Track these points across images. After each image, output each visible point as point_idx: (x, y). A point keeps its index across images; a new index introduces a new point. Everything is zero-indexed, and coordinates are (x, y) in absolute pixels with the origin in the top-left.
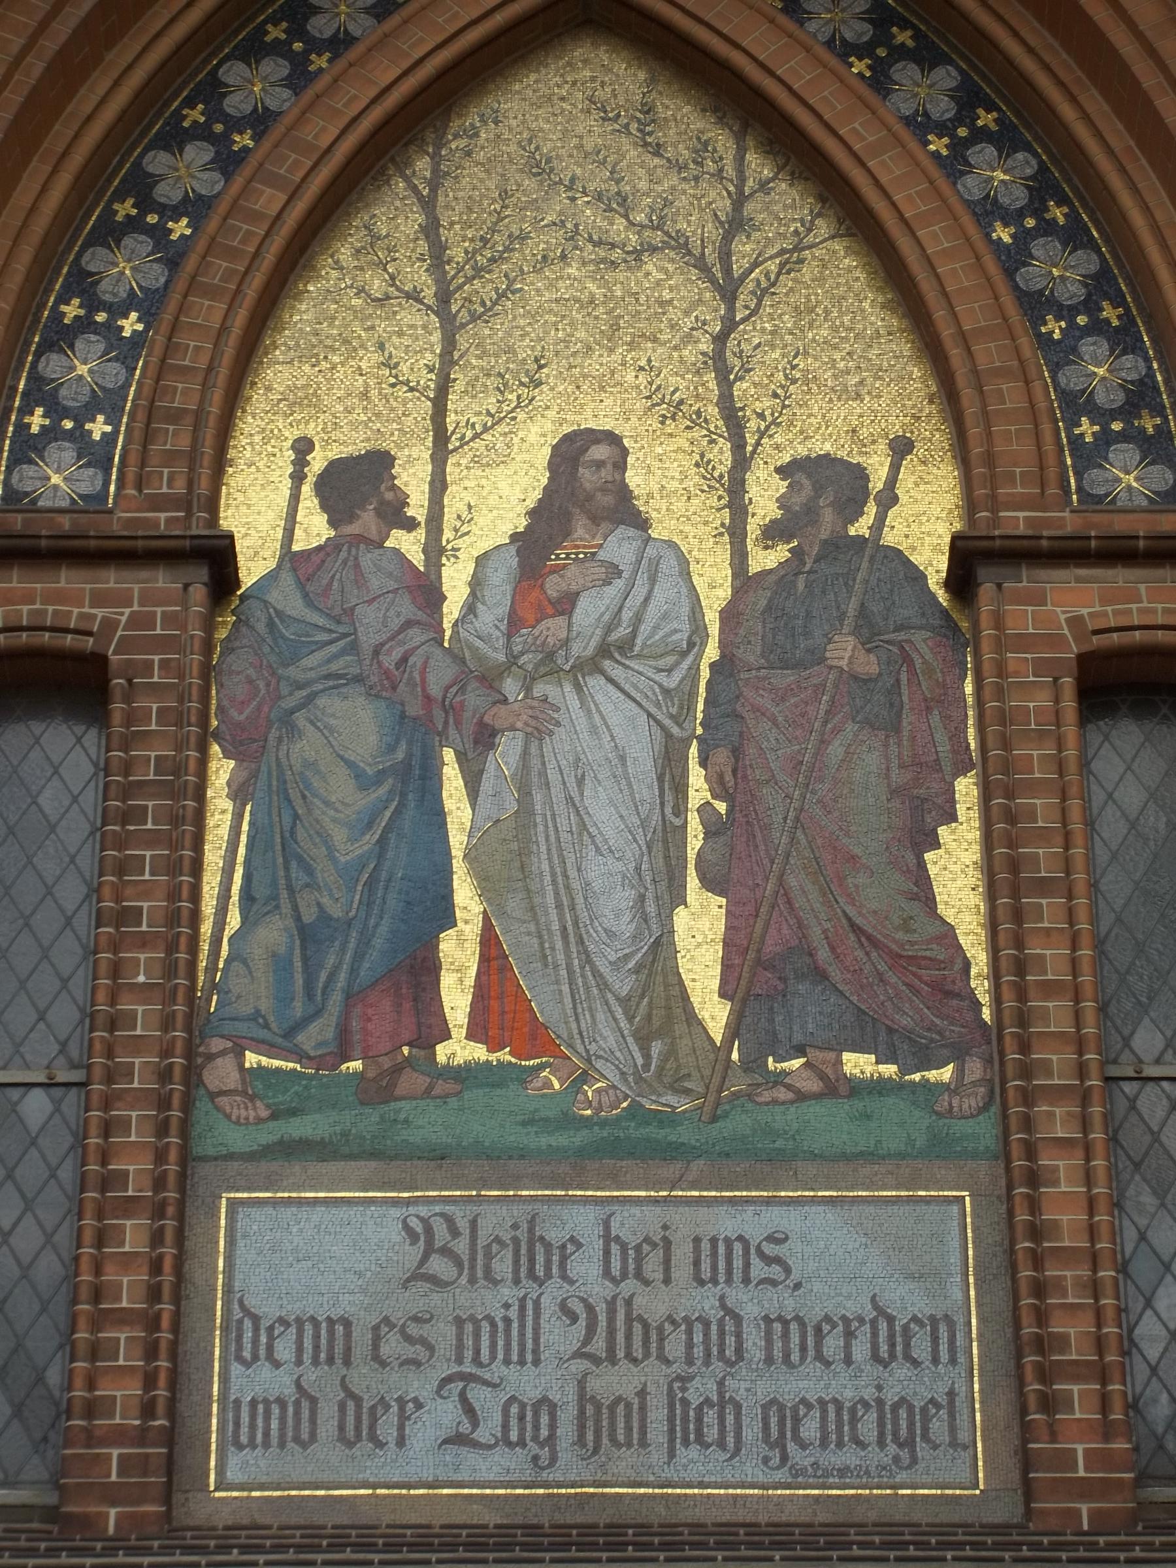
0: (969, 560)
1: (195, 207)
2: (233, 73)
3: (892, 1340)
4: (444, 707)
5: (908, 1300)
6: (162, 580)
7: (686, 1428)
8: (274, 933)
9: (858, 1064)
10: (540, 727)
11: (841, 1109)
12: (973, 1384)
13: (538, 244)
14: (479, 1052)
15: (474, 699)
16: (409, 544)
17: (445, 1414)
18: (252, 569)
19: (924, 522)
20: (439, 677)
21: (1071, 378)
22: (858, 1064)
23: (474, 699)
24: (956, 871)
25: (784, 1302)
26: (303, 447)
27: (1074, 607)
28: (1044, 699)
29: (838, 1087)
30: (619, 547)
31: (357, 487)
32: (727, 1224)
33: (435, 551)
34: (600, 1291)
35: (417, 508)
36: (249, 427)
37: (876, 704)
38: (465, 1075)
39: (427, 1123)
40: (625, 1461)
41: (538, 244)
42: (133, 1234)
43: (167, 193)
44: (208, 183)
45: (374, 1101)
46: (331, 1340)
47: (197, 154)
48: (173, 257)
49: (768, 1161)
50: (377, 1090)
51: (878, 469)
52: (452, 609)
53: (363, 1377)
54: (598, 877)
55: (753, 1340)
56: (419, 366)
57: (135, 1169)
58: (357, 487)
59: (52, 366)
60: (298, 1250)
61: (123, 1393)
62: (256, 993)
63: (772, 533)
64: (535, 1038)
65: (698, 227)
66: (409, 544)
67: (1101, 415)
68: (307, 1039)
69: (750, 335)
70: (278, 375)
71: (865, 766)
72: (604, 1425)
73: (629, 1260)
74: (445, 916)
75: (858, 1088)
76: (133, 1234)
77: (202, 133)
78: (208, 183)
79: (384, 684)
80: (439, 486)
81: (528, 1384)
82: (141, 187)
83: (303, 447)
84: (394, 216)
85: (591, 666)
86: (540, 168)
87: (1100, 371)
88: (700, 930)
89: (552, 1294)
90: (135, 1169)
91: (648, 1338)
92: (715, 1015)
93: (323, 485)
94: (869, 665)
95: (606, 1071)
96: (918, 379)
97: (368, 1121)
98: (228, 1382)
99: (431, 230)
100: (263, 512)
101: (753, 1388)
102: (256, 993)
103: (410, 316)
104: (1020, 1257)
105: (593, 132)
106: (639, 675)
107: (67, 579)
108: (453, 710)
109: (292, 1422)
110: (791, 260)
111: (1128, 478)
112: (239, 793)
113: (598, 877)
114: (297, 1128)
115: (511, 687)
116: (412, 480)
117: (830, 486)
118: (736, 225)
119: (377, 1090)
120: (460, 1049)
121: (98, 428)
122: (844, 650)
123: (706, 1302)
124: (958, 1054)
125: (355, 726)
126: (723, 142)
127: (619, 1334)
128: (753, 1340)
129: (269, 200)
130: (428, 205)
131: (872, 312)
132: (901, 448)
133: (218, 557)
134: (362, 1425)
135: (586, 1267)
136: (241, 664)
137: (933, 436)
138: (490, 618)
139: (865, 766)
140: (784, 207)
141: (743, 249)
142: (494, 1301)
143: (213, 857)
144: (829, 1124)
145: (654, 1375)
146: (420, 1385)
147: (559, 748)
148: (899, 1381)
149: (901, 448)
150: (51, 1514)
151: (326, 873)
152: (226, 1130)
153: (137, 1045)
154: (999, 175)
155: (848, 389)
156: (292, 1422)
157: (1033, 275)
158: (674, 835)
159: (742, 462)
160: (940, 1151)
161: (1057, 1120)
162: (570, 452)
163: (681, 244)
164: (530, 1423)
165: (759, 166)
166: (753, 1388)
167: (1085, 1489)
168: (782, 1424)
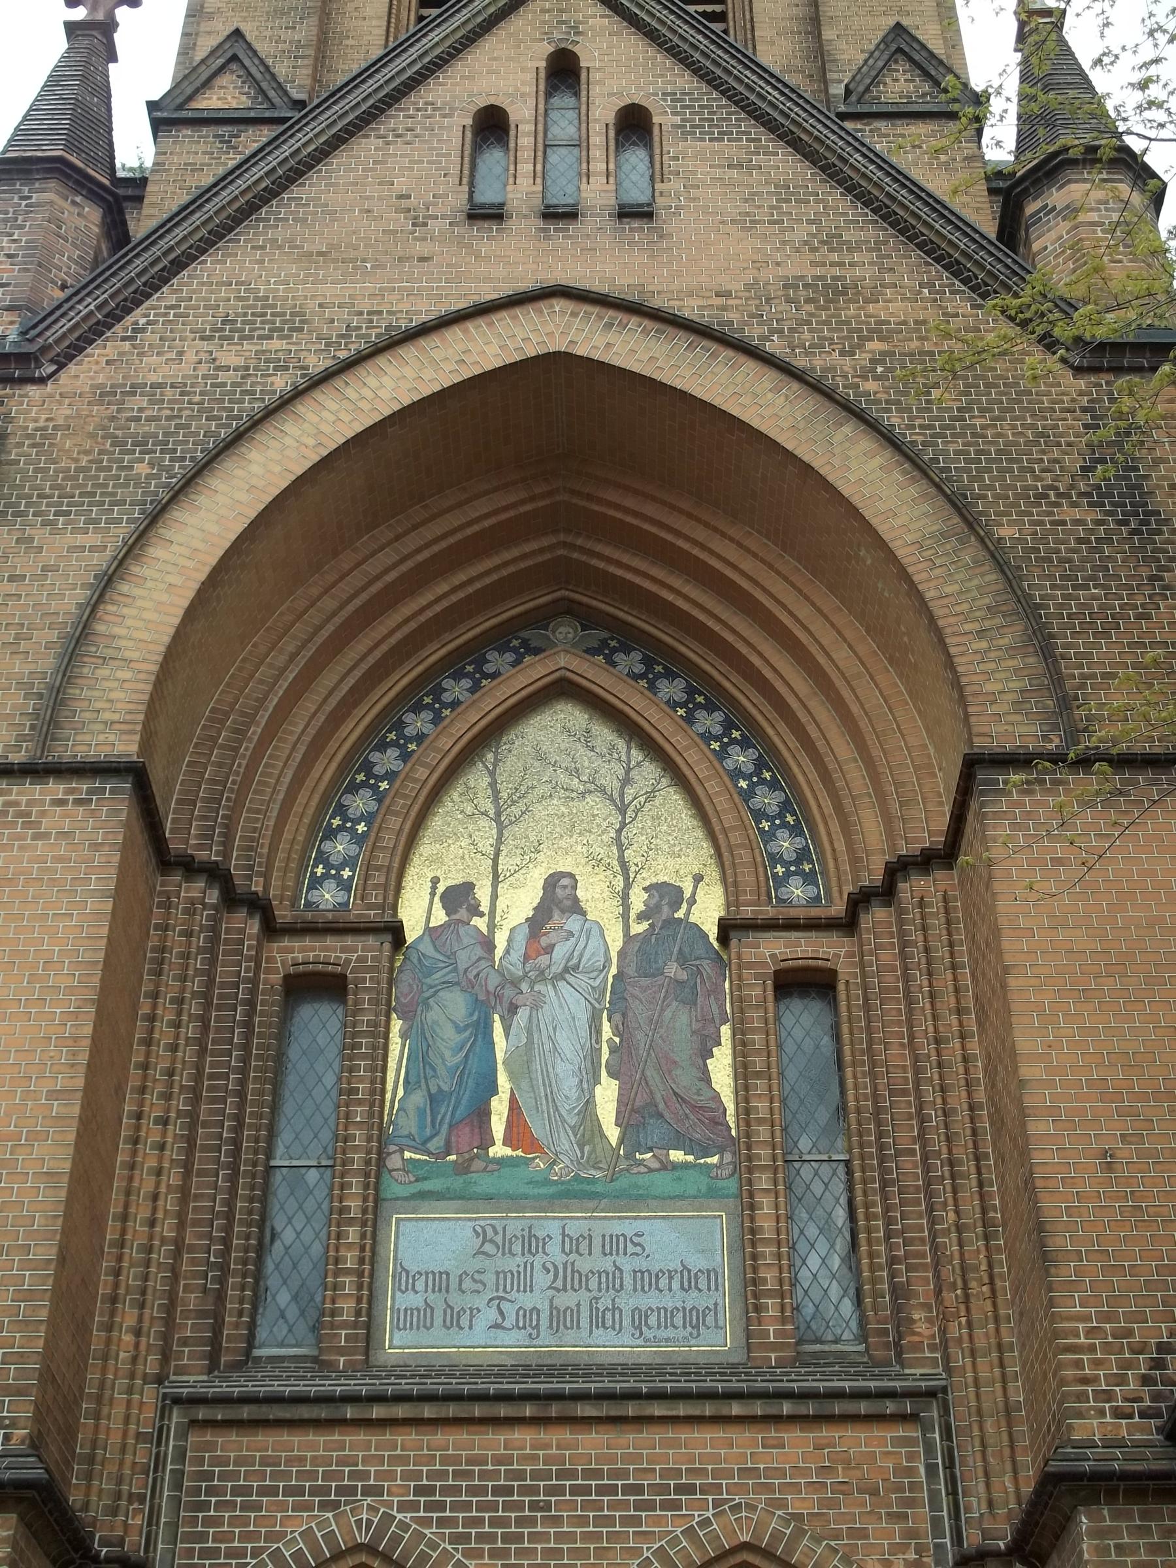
0: (726, 929)
1: (390, 776)
2: (409, 718)
3: (690, 1279)
5: (697, 1262)
6: (371, 941)
7: (598, 1321)
8: (418, 1098)
9: (676, 1156)
10: (536, 1007)
11: (667, 1176)
13: (539, 791)
14: (508, 1151)
15: (508, 992)
16: (481, 923)
17: (492, 1315)
18: (411, 936)
19: (708, 911)
20: (493, 981)
21: (773, 847)
22: (676, 1156)
23: (508, 992)
24: (721, 1068)
25: (640, 1263)
26: (435, 881)
27: (775, 949)
28: (759, 991)
29: (667, 1166)
30: (573, 923)
31: (458, 898)
32: (617, 1228)
33: (492, 926)
34: (560, 1259)
35: (485, 907)
36: (412, 872)
37: (685, 992)
38: (501, 1162)
39: (485, 1183)
40: (570, 1336)
41: (539, 791)
42: (353, 1234)
43: (378, 770)
44: (397, 765)
46: (440, 1281)
47: (393, 753)
48: (380, 797)
49: (635, 1199)
50: (462, 1169)
51: (687, 887)
52: (499, 952)
53: (455, 1299)
54: (561, 1072)
55: (628, 1281)
56: (487, 844)
57: (354, 1205)
59: (327, 846)
60: (426, 1241)
61: (348, 1305)
62: (409, 1125)
63: (641, 917)
64: (533, 1145)
65: (610, 782)
66: (481, 923)
67: (786, 864)
68: (432, 1146)
69: (631, 831)
70: (426, 849)
71: (681, 1020)
72: (561, 1319)
73: (574, 1245)
74: (494, 1091)
75: (675, 1166)
76: (353, 1234)
77: (394, 744)
78: (397, 765)
79: (468, 985)
80: (494, 897)
81: (527, 1301)
82: (367, 767)
83: (435, 881)
84: (477, 778)
85: (560, 977)
86: (541, 757)
87: (786, 844)
88: (607, 1094)
89: (538, 1260)
90: (354, 1205)
91: (583, 1279)
92: (613, 1134)
93: (442, 898)
94: (683, 976)
95: (564, 1157)
96: (706, 848)
97: (457, 1183)
98: (395, 1300)
99: (493, 785)
100: (417, 911)
101: (628, 1302)
102: (409, 1125)
103: (484, 822)
104: (747, 1240)
105: (564, 741)
106: (581, 980)
107: (330, 941)
108: (498, 997)
109: (422, 1318)
110: (650, 795)
111: (797, 891)
112: (404, 1035)
113: (561, 1072)
114: (427, 1186)
115: (524, 987)
116: (483, 895)
117: (667, 896)
118: (626, 781)
119: (462, 1169)
120: (499, 1150)
121: (346, 873)
122: (672, 969)
123: (607, 1264)
124: (721, 1151)
126: (621, 744)
127: (568, 1278)
128: (628, 1281)
129: (422, 773)
130: (492, 774)
131: (686, 818)
132: (698, 879)
133: (396, 932)
134: (453, 1320)
135: (554, 1248)
136: (406, 978)
137: (712, 873)
138: (516, 956)
139: (681, 1020)
140: (648, 772)
141: (630, 792)
142: (513, 1264)
143: (392, 1064)
144: (663, 1183)
145: (584, 1297)
146: (480, 1302)
147: (545, 1014)
148: (693, 1299)
149: (698, 879)
150: (315, 1360)
151: (441, 1071)
152: (394, 1187)
153: (356, 1149)
156: (422, 1318)
157: (756, 803)
158: (595, 1053)
159: (628, 885)
160: (712, 1193)
161: (763, 1181)
162: (552, 882)
163: (602, 790)
164: (528, 1319)
165: (636, 755)
166: (628, 1302)
167: (774, 1347)
168: (641, 1318)
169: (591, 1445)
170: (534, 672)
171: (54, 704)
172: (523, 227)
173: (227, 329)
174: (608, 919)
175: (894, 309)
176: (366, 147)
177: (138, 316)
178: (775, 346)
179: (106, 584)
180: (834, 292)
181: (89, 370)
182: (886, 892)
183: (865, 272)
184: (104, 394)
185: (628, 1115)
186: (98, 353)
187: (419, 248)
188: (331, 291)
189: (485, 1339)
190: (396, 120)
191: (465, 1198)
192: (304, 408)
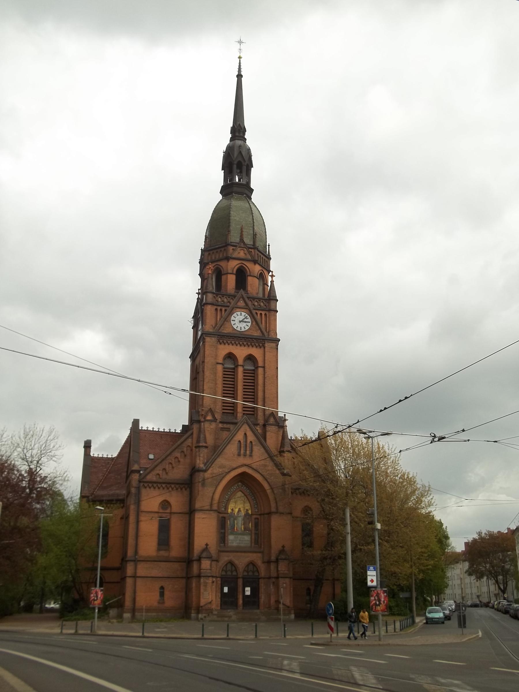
3: (248, 541)
4: (235, 518)
19: (250, 512)
27: (254, 516)
28: (253, 520)
31: (232, 510)
45: (233, 532)
54: (239, 524)
58: (232, 510)
60: (231, 537)
88: (243, 526)
95: (240, 532)
100: (230, 511)
117: (247, 510)
125: (232, 519)
154: (255, 502)
155: (248, 506)
169: (243, 554)
171: (211, 505)
172: (242, 456)
173: (220, 467)
174: (243, 513)
175: (270, 468)
176: (229, 445)
177: (213, 465)
178: (261, 472)
179: (214, 493)
180: (265, 466)
181: (209, 471)
182: (264, 514)
183: (268, 464)
184: (212, 474)
185: (245, 528)
186: (211, 469)
189: (235, 544)
190: (232, 442)
191: (234, 534)
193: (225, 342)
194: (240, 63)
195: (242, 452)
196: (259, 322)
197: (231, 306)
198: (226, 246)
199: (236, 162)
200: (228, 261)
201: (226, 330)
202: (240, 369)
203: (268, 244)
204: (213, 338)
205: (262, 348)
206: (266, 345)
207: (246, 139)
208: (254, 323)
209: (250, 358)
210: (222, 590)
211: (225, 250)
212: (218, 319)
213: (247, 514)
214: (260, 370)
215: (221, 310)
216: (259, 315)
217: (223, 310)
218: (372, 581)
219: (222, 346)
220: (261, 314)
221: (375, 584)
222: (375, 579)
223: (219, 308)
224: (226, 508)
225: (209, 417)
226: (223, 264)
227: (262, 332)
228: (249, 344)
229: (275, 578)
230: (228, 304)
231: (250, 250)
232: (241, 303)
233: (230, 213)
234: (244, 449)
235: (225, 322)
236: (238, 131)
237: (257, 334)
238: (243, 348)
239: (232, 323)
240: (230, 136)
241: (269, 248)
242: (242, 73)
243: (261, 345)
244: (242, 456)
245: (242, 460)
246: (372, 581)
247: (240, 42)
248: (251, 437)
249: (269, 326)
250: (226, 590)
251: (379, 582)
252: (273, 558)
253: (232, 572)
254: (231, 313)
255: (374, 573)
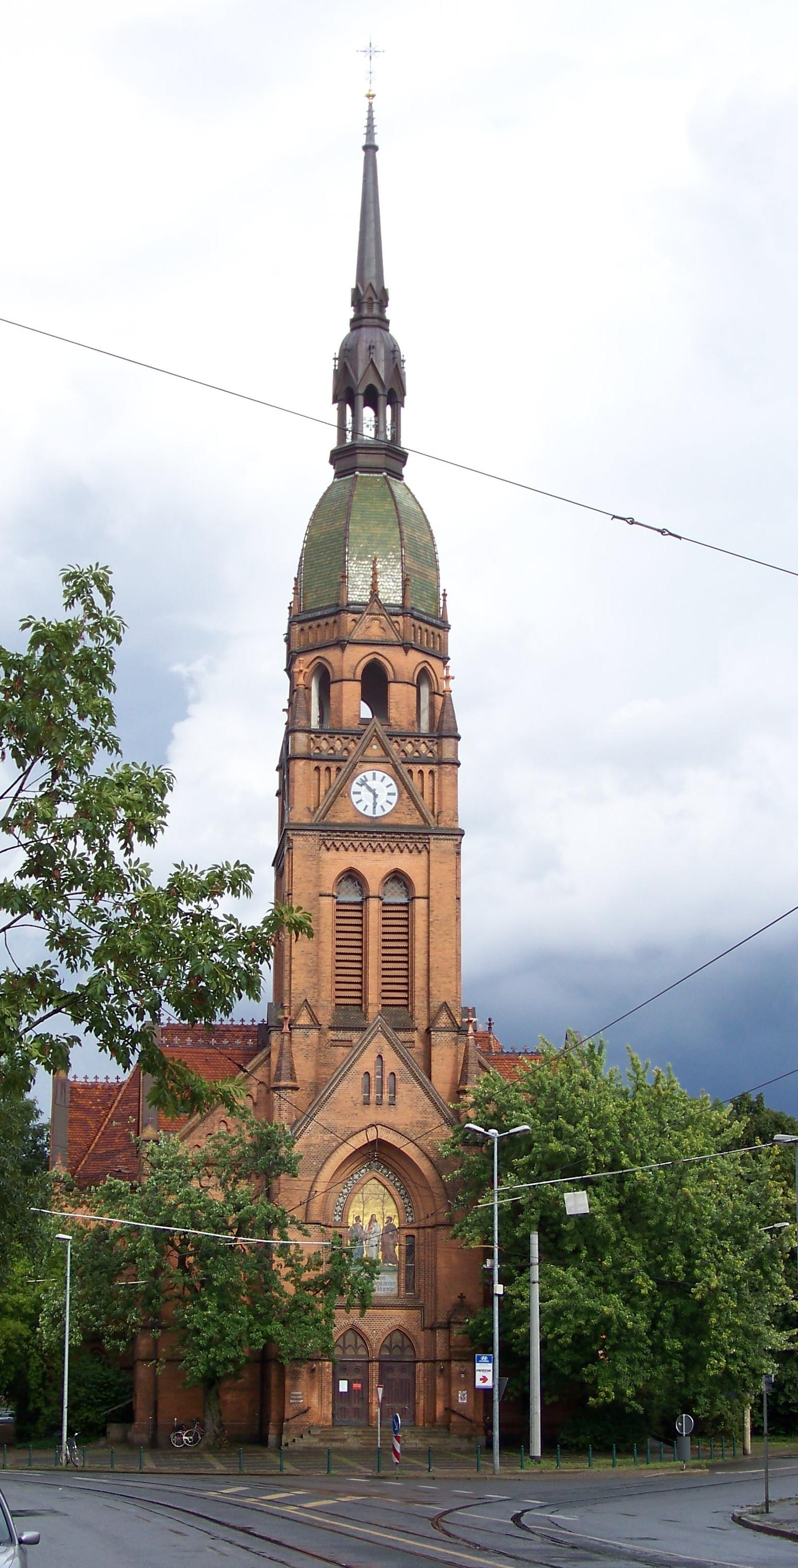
12: (395, 1287)
19: (396, 1222)
27: (406, 1232)
28: (403, 1239)
31: (357, 1218)
58: (357, 1218)
88: (381, 1253)
100: (351, 1221)
116: (361, 1218)
117: (390, 1218)
155: (391, 1210)
160: (395, 1270)
170: (370, 1176)
172: (373, 1106)
174: (380, 1226)
182: (424, 1228)
184: (307, 1146)
187: (356, 1112)
188: (340, 1122)
190: (350, 1075)
192: (338, 1150)
193: (338, 844)
194: (370, 111)
195: (373, 1096)
196: (417, 791)
197: (350, 760)
198: (338, 613)
199: (361, 390)
200: (343, 649)
201: (343, 817)
202: (374, 905)
203: (442, 592)
204: (310, 839)
205: (424, 853)
206: (432, 847)
207: (387, 322)
208: (405, 795)
209: (397, 877)
210: (336, 1386)
211: (335, 622)
212: (322, 793)
213: (389, 1228)
214: (420, 904)
215: (328, 769)
216: (415, 775)
217: (333, 769)
218: (484, 1379)
219: (332, 854)
220: (421, 772)
221: (489, 1384)
222: (489, 1376)
223: (323, 766)
224: (344, 1215)
225: (304, 1020)
226: (332, 655)
227: (422, 815)
228: (393, 845)
229: (444, 1361)
230: (345, 753)
231: (394, 619)
232: (375, 750)
233: (347, 530)
234: (378, 1091)
235: (339, 798)
236: (369, 302)
237: (413, 820)
238: (378, 855)
239: (355, 798)
240: (350, 313)
241: (444, 600)
242: (377, 141)
243: (420, 846)
244: (373, 1106)
245: (372, 1114)
246: (484, 1379)
247: (371, 52)
248: (392, 1063)
249: (440, 801)
250: (343, 1386)
251: (497, 1382)
252: (442, 1319)
253: (356, 1348)
254: (349, 777)
255: (489, 1366)
